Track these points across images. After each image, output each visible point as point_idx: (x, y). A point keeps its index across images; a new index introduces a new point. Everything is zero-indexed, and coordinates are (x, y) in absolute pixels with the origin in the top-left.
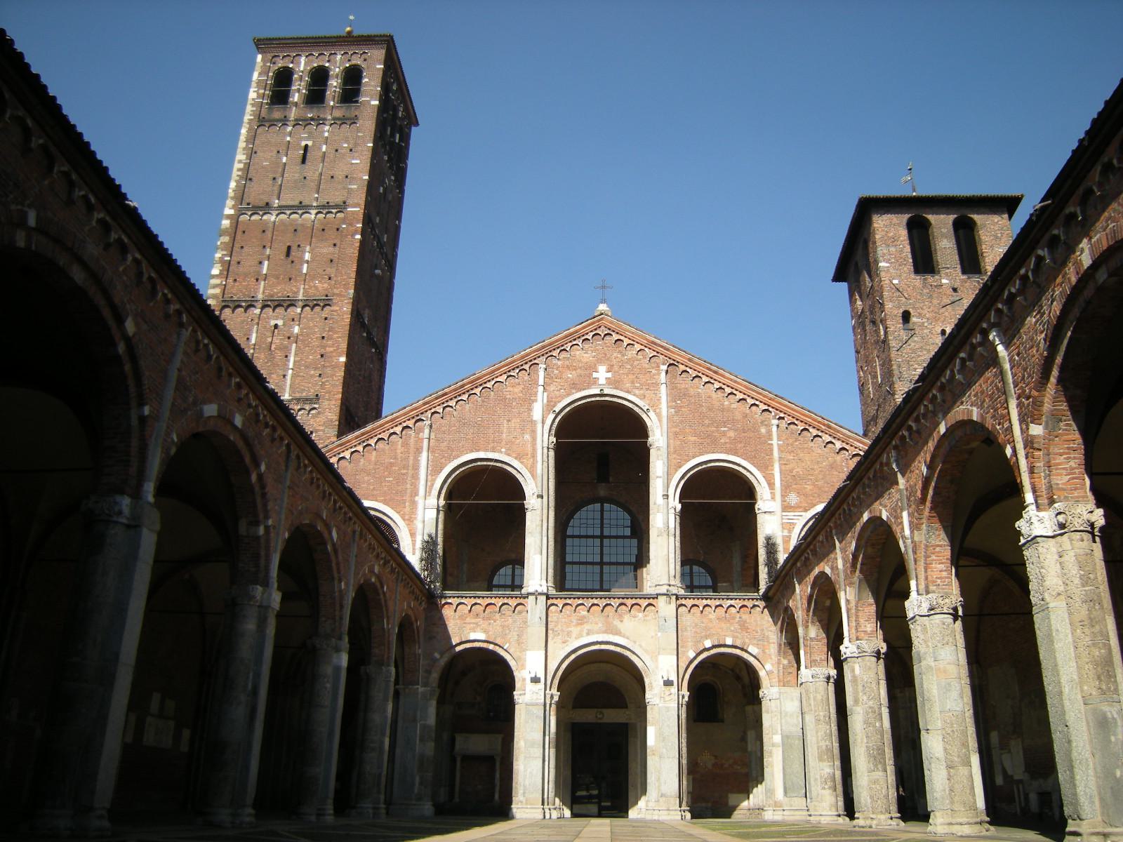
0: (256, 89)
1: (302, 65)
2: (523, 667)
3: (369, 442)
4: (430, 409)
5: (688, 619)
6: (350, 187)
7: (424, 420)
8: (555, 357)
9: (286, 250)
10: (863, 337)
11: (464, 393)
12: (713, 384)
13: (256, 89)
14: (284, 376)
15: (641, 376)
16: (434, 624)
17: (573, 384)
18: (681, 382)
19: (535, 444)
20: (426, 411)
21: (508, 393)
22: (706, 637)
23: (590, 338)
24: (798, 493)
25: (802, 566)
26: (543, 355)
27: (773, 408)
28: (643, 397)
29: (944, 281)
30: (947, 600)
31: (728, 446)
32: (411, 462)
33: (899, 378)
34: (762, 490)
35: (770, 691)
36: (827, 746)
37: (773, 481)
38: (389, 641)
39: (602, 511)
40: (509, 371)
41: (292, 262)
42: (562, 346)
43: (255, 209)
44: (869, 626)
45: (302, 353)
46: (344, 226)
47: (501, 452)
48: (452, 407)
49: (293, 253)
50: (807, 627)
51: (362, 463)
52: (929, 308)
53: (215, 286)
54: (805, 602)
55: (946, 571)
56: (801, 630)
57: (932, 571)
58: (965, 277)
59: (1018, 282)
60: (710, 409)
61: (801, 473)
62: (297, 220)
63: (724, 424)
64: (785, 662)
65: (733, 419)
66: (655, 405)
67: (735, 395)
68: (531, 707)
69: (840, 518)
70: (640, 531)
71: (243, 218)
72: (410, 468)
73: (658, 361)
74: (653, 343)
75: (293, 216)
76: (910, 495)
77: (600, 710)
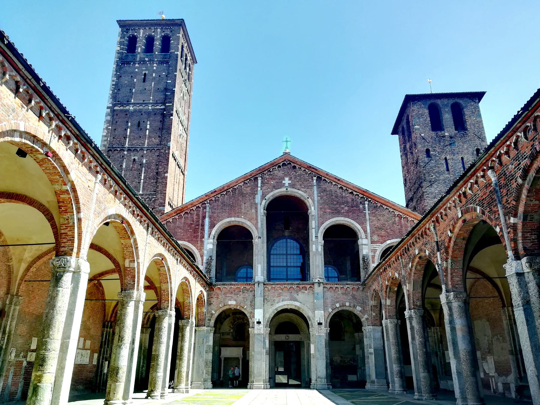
1: (141, 34)
2: (254, 317)
3: (181, 214)
4: (209, 198)
5: (329, 294)
6: (167, 93)
7: (205, 204)
10: (406, 160)
11: (224, 191)
13: (119, 45)
14: (139, 183)
16: (212, 298)
17: (274, 186)
18: (323, 185)
19: (257, 214)
20: (207, 200)
21: (244, 191)
22: (337, 302)
23: (281, 165)
25: (383, 271)
26: (260, 173)
28: (306, 192)
29: (446, 134)
30: (461, 296)
32: (200, 223)
33: (424, 180)
34: (361, 233)
35: (367, 329)
36: (397, 357)
38: (192, 308)
39: (287, 242)
40: (245, 181)
41: (141, 129)
43: (122, 105)
44: (418, 302)
45: (147, 172)
46: (165, 112)
47: (241, 217)
48: (219, 197)
50: (386, 300)
51: (177, 224)
52: (439, 147)
54: (384, 287)
55: (460, 281)
56: (383, 301)
57: (453, 281)
58: (457, 132)
59: (505, 148)
60: (336, 197)
61: (379, 226)
62: (143, 109)
63: (343, 204)
64: (374, 314)
66: (311, 196)
67: (348, 190)
68: (257, 336)
69: (403, 252)
70: (305, 252)
71: (116, 108)
72: (200, 226)
73: (312, 175)
74: (310, 167)
75: (141, 107)
76: (441, 244)
77: (287, 335)
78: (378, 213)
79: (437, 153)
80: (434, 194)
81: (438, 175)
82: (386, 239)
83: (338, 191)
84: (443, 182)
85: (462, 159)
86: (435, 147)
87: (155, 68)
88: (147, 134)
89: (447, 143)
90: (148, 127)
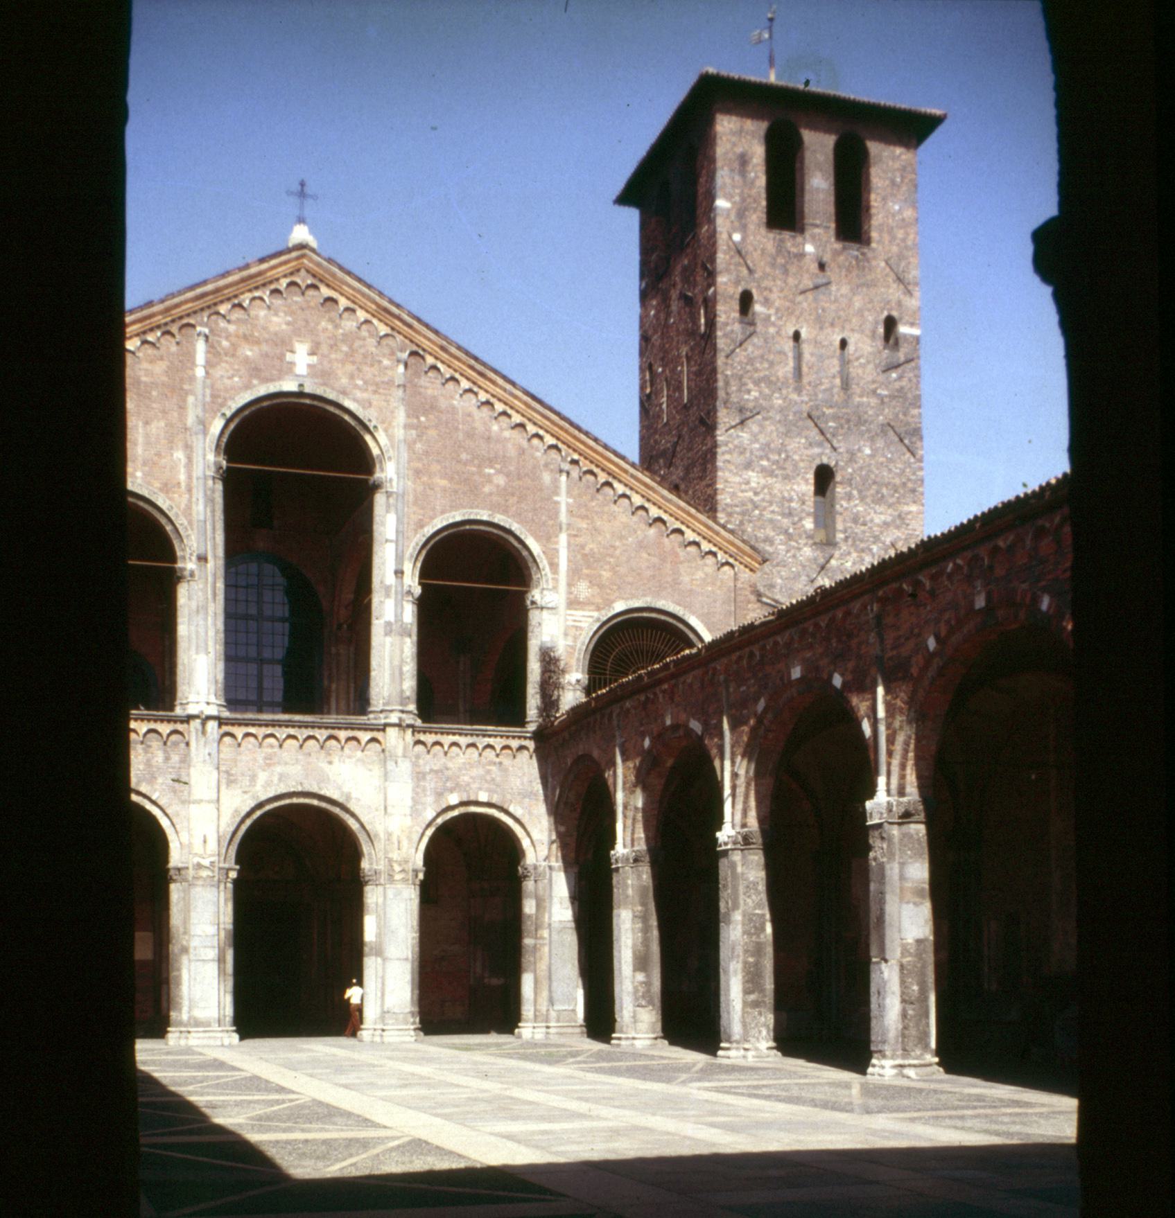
8: (224, 317)
12: (476, 394)
15: (366, 368)
18: (428, 385)
24: (590, 582)
27: (564, 443)
29: (809, 248)
31: (495, 498)
37: (556, 560)
42: (236, 296)
61: (596, 550)
63: (491, 462)
65: (504, 456)
78: (596, 509)
79: (772, 311)
80: (748, 455)
81: (767, 391)
82: (612, 598)
83: (476, 418)
84: (778, 418)
85: (844, 343)
86: (771, 291)
89: (808, 283)
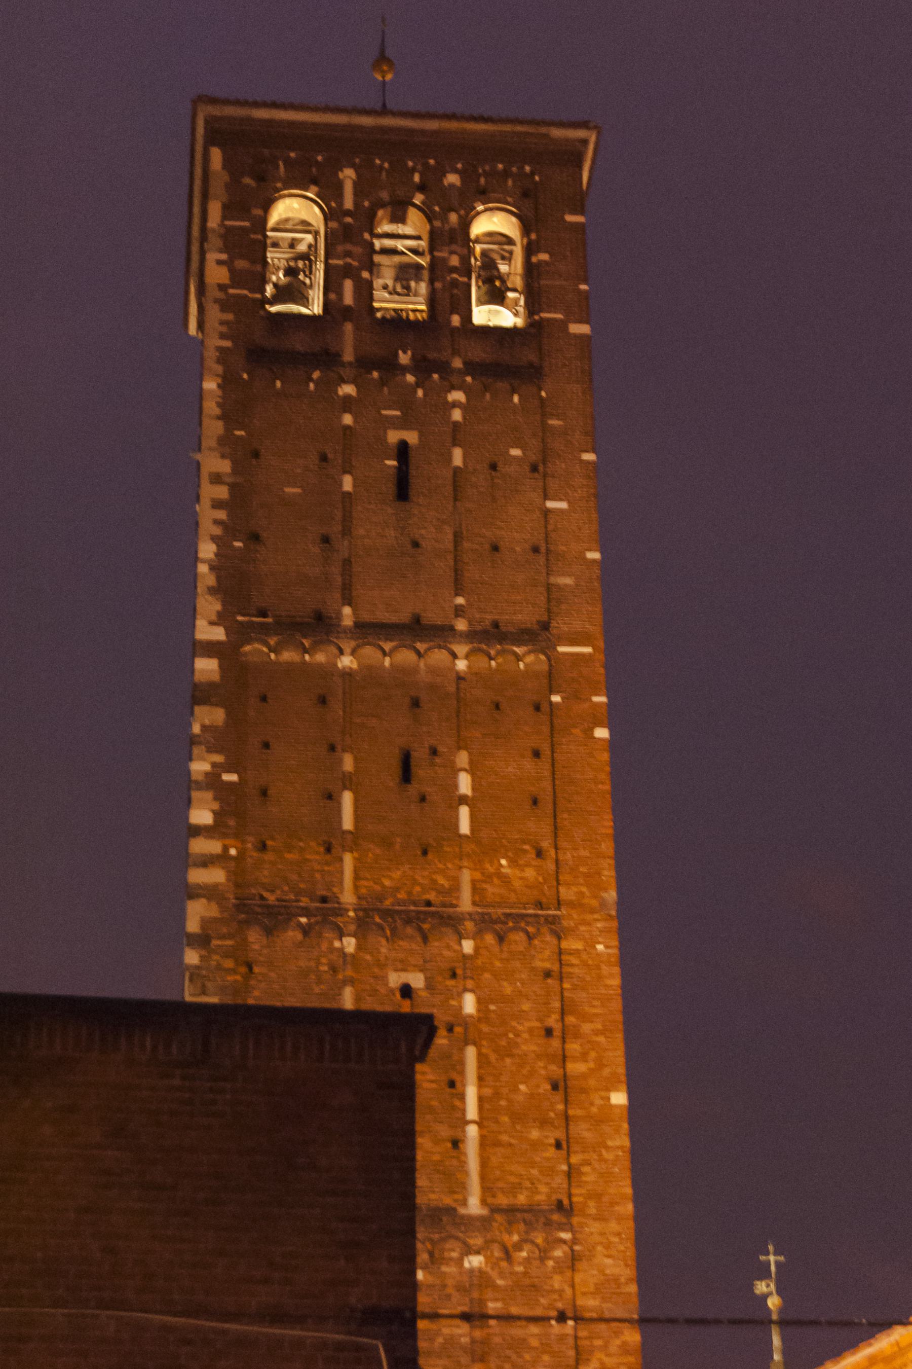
0: (224, 257)
9: (395, 763)
13: (224, 257)
14: (456, 1143)
41: (423, 799)
46: (556, 699)
49: (420, 772)
53: (206, 862)
87: (457, 415)
88: (465, 827)
90: (465, 783)
